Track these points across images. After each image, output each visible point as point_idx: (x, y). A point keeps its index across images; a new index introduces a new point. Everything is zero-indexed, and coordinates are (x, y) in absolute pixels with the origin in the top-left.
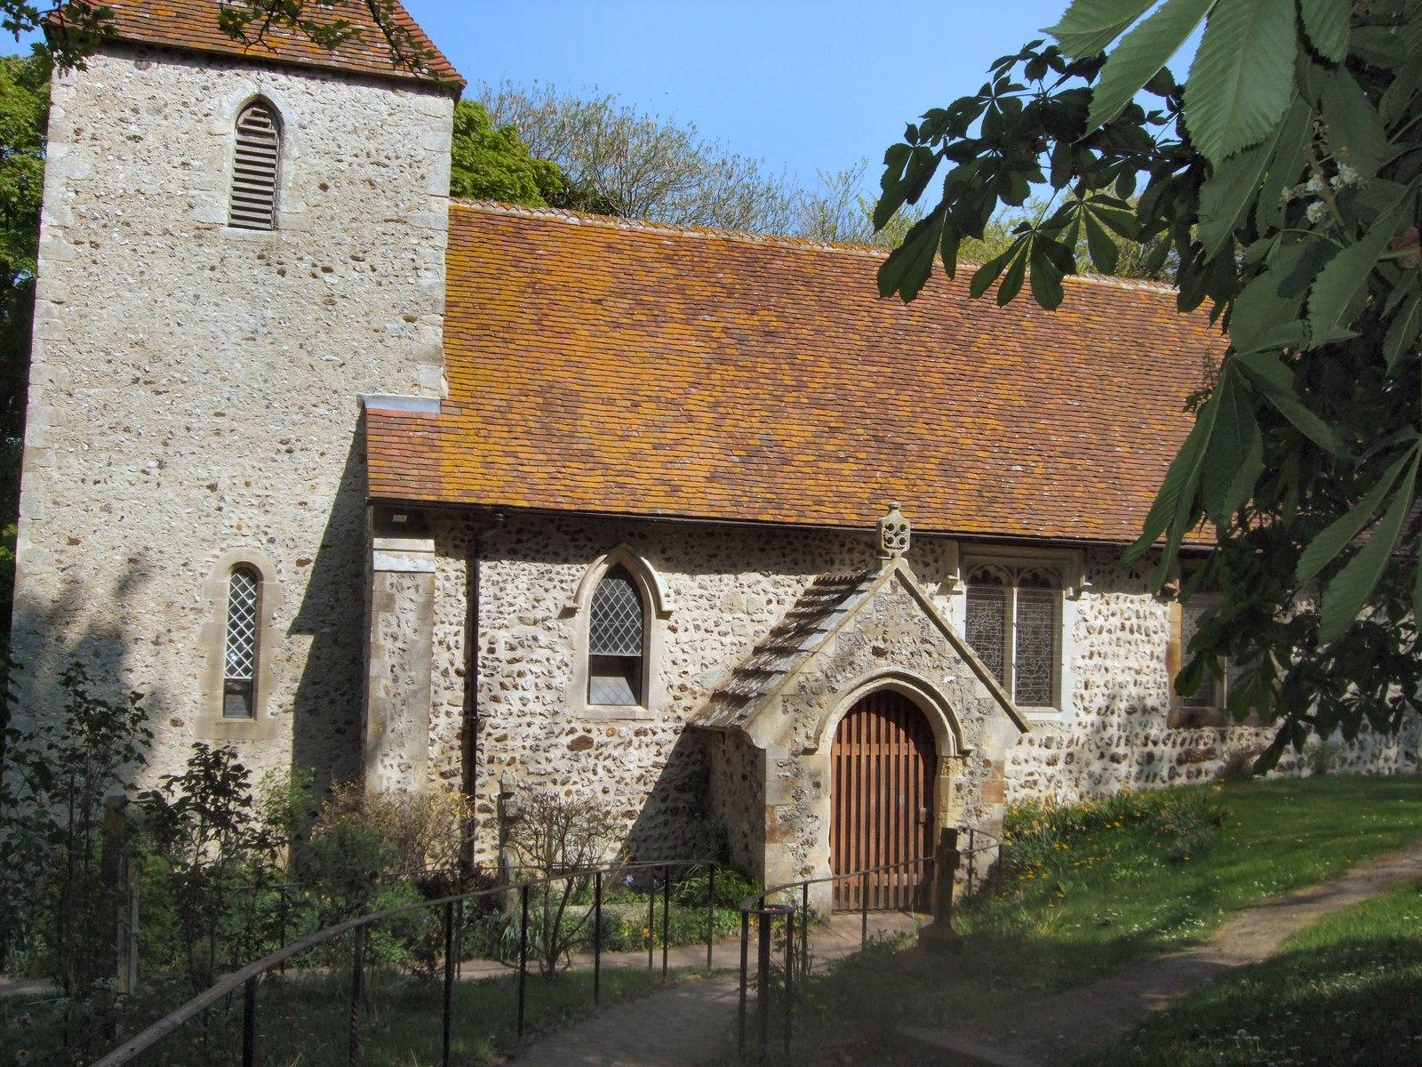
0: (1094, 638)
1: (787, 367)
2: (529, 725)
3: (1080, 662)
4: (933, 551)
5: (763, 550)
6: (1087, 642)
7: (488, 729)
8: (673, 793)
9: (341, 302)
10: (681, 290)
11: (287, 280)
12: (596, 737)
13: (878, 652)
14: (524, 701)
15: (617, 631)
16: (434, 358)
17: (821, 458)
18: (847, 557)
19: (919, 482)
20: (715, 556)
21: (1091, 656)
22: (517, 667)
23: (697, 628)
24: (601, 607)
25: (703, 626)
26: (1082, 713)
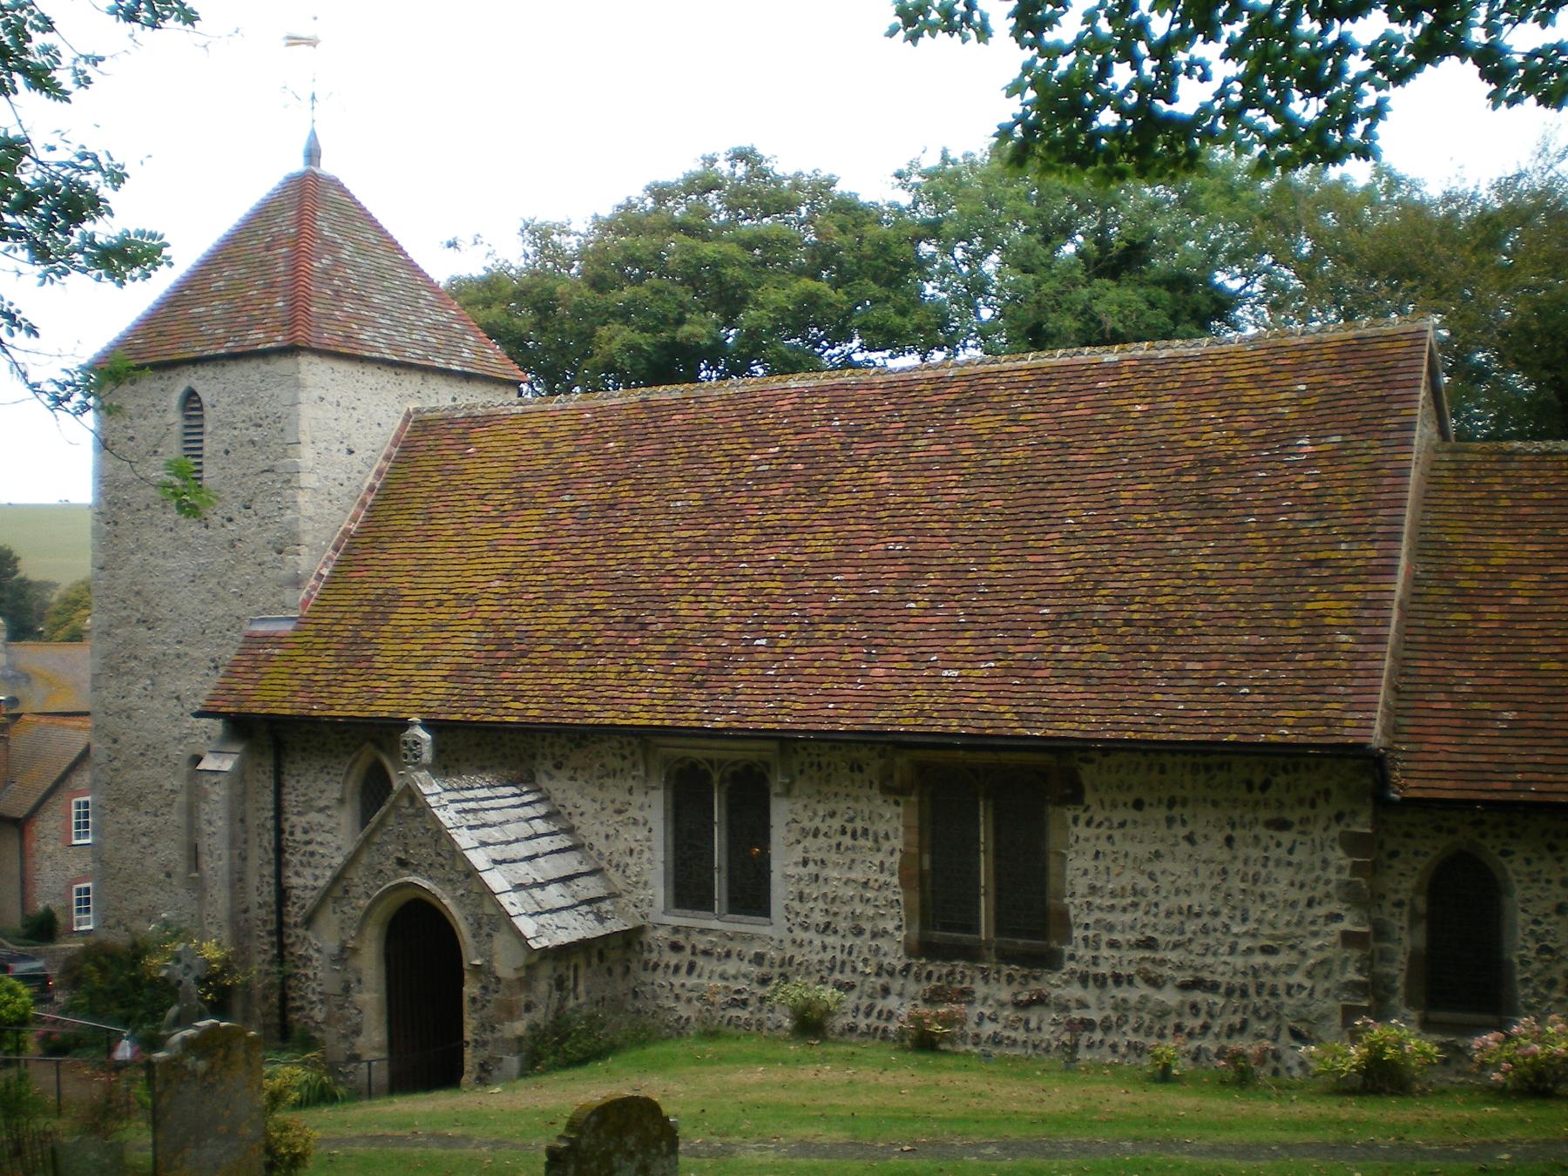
0: (808, 841)
3: (791, 870)
4: (630, 743)
5: (478, 745)
9: (239, 544)
18: (548, 751)
21: (805, 863)
22: (310, 848)
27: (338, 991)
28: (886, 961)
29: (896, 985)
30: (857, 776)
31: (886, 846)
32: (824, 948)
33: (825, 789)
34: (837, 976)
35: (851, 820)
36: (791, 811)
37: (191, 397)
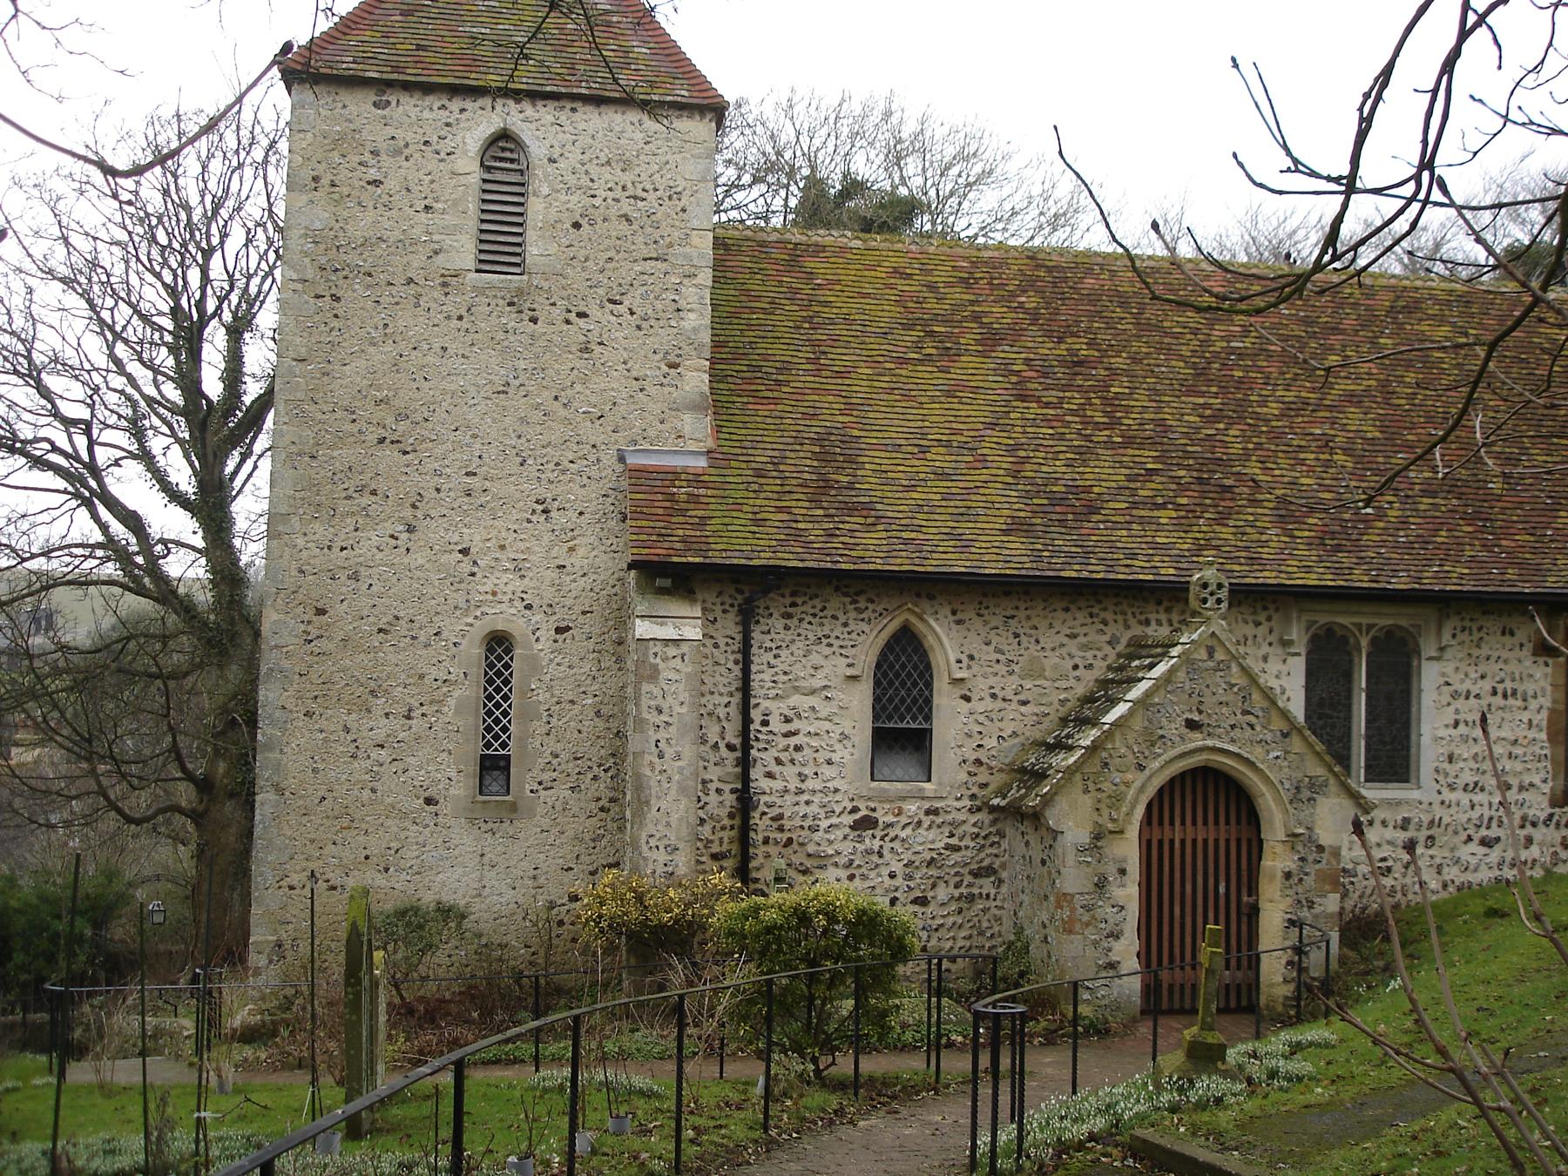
0: (1459, 703)
1: (1097, 401)
2: (807, 803)
3: (1442, 733)
6: (1452, 708)
7: (762, 808)
8: (968, 879)
10: (976, 318)
11: (540, 327)
12: (883, 818)
13: (1192, 725)
14: (802, 777)
15: (903, 701)
16: (694, 407)
17: (1135, 505)
18: (1163, 617)
19: (1249, 530)
20: (1013, 617)
21: (1456, 724)
22: (793, 741)
23: (994, 696)
24: (885, 675)
25: (1001, 694)
26: (1445, 791)
27: (1091, 887)
28: (1531, 813)
29: (1538, 834)
30: (1507, 638)
31: (1533, 705)
32: (1473, 807)
33: (1475, 652)
34: (1484, 832)
35: (1502, 681)
36: (1443, 675)
37: (503, 143)
